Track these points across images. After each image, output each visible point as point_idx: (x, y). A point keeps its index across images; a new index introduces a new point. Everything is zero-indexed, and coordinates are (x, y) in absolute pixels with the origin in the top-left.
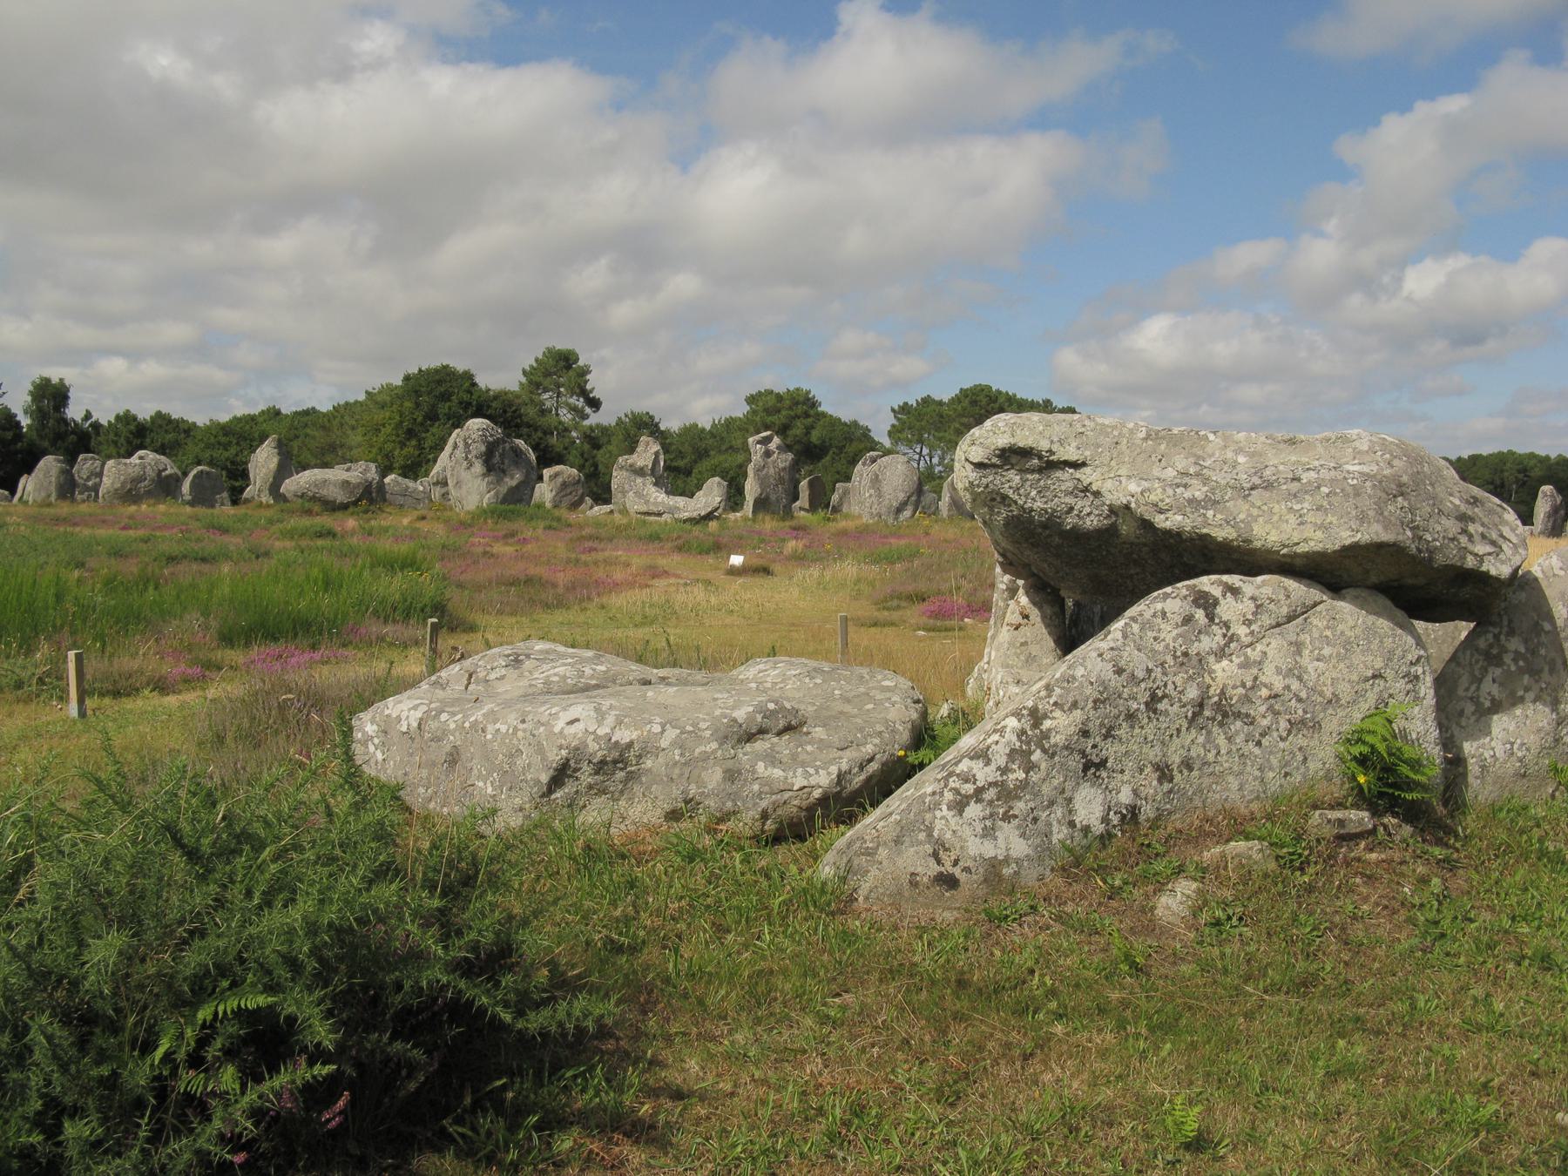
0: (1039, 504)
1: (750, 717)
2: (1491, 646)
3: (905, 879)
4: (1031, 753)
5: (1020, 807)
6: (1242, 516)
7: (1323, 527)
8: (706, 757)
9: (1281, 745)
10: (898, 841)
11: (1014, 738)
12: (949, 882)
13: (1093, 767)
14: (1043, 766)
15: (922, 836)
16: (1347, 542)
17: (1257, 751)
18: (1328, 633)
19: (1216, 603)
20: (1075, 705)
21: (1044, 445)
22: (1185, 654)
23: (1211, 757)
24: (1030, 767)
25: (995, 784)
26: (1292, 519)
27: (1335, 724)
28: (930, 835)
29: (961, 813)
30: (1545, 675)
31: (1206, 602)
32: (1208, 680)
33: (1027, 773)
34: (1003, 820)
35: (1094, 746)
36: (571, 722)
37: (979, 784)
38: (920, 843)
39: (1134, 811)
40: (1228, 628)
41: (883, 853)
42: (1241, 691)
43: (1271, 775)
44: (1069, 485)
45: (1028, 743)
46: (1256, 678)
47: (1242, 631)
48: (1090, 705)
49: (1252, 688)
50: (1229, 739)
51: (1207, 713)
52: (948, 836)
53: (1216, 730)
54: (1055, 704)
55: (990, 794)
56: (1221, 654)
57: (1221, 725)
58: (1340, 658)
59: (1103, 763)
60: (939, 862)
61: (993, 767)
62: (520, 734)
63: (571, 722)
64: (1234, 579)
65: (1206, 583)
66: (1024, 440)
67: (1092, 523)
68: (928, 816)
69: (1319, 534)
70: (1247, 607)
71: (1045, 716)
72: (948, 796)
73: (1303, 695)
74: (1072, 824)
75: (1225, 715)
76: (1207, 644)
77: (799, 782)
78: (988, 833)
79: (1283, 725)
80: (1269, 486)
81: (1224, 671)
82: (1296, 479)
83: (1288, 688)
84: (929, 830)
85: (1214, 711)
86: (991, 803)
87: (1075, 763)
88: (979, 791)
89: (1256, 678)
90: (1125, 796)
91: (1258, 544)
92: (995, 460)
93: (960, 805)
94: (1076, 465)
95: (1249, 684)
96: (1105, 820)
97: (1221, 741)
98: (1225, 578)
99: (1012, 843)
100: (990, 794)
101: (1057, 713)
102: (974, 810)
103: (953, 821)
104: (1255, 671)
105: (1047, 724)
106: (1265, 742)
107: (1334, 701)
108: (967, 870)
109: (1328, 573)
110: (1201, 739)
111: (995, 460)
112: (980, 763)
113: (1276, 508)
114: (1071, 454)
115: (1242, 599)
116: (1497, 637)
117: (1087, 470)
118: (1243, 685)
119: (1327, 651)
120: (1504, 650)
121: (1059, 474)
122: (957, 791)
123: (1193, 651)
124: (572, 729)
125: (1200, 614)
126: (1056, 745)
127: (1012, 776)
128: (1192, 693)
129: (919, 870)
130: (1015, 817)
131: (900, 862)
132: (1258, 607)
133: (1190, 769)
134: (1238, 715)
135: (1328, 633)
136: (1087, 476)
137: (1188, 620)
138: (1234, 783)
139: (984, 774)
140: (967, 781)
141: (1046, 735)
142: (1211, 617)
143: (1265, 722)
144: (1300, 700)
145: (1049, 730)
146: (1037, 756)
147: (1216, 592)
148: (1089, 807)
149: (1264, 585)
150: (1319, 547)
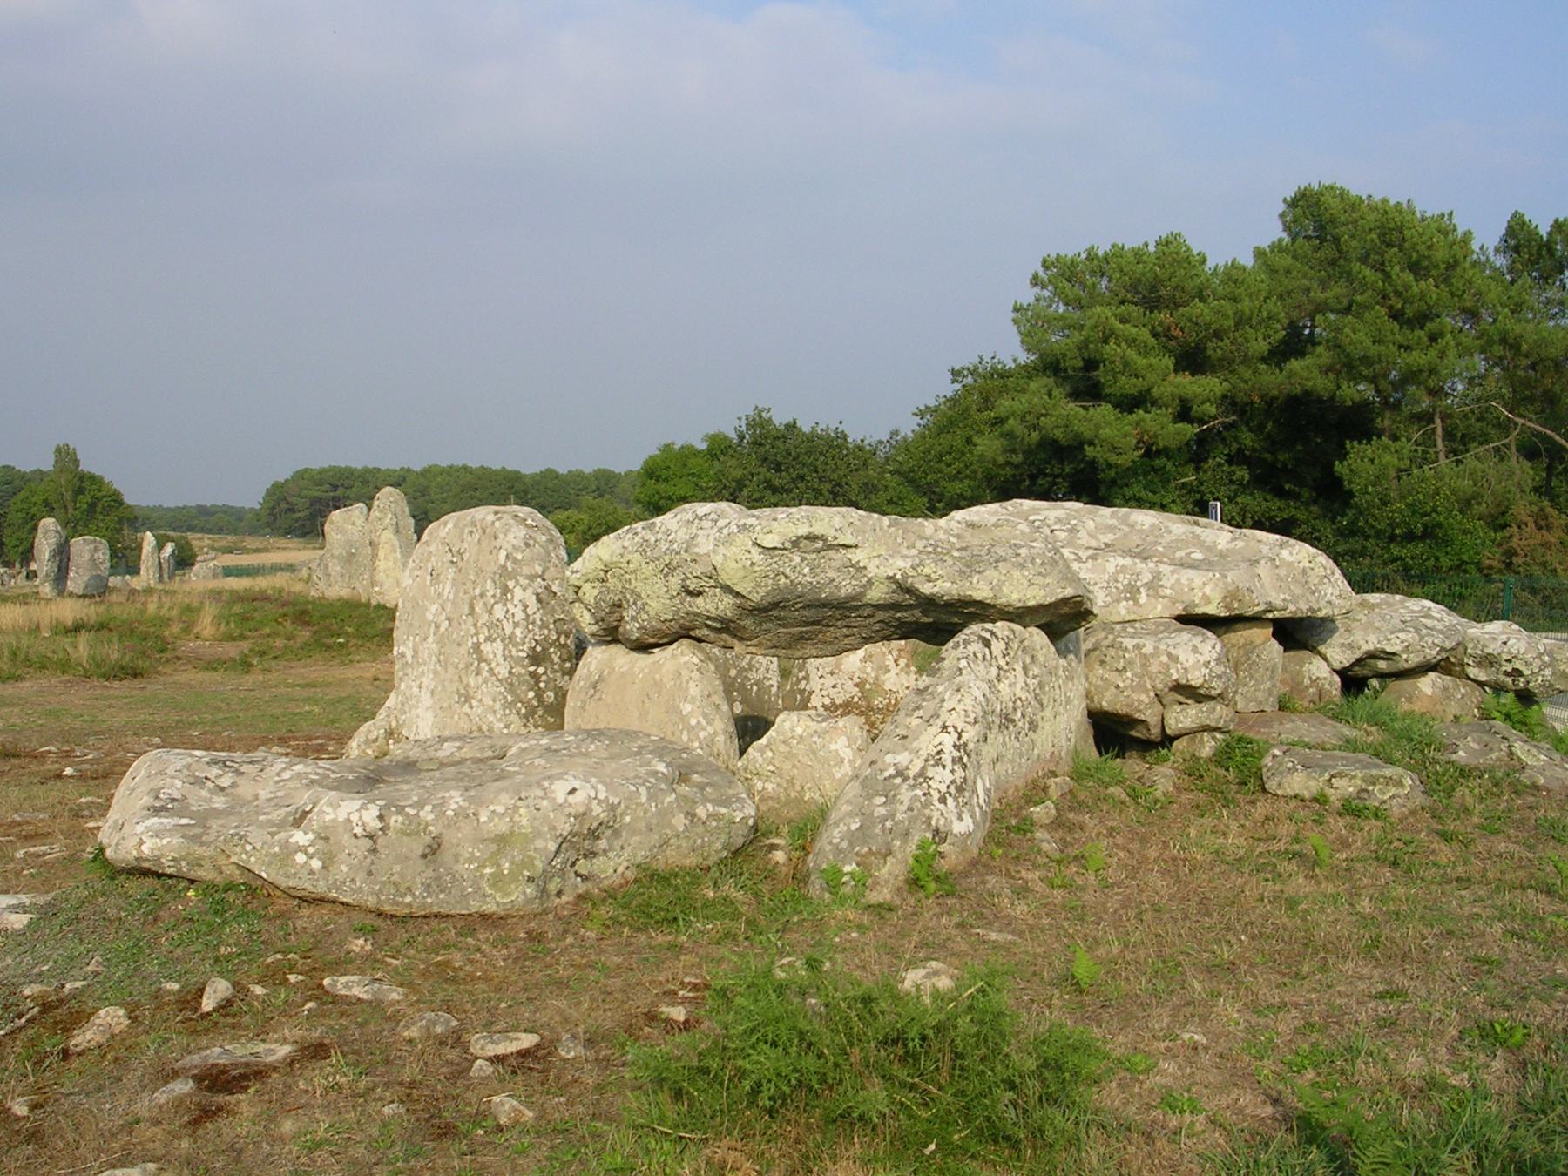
36: (573, 791)
47: (1002, 662)
63: (573, 791)
64: (989, 626)
65: (975, 628)
66: (817, 529)
70: (1002, 645)
72: (936, 795)
92: (788, 545)
105: (965, 736)
111: (788, 545)
121: (831, 553)
141: (965, 745)
147: (988, 635)
149: (1001, 627)
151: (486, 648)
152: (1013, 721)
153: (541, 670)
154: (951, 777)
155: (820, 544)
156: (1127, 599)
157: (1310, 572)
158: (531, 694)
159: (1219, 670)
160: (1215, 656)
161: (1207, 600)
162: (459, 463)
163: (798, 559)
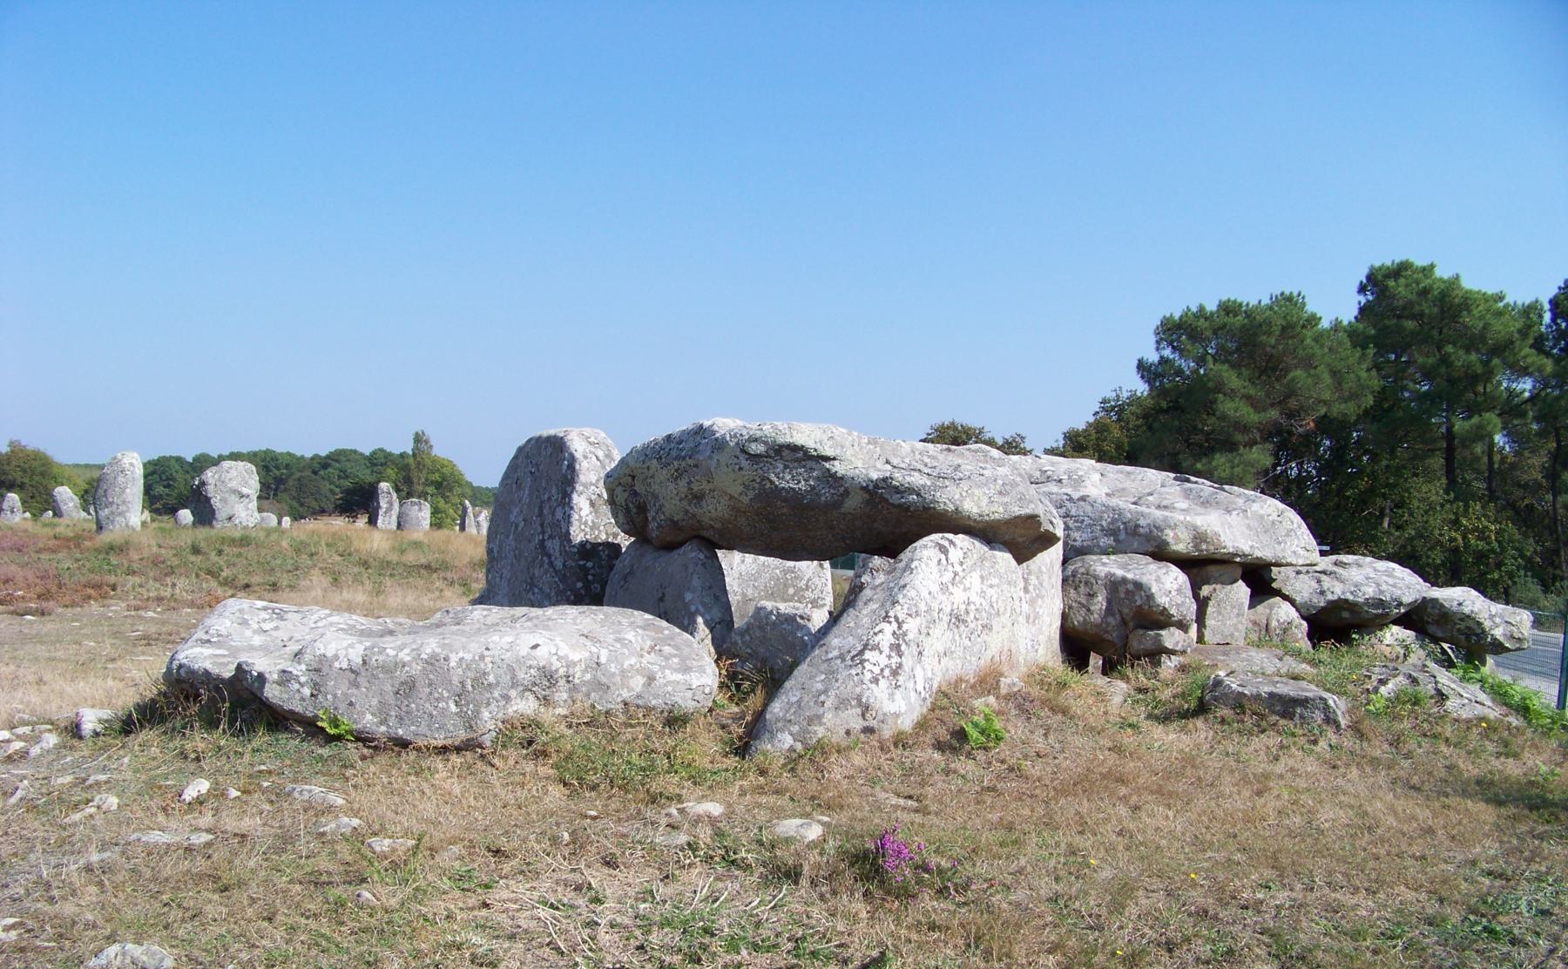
26: (986, 500)
36: (535, 647)
47: (958, 568)
55: (887, 672)
62: (488, 660)
63: (535, 647)
65: (936, 537)
70: (960, 554)
92: (771, 453)
93: (875, 681)
94: (827, 459)
105: (905, 627)
111: (771, 453)
117: (836, 463)
121: (810, 464)
124: (534, 652)
141: (905, 634)
146: (903, 647)
147: (946, 544)
149: (961, 540)
151: (548, 544)
152: (964, 621)
153: (590, 564)
154: (887, 662)
155: (800, 454)
158: (579, 585)
159: (1179, 600)
161: (1177, 539)
162: (658, 434)
163: (781, 466)
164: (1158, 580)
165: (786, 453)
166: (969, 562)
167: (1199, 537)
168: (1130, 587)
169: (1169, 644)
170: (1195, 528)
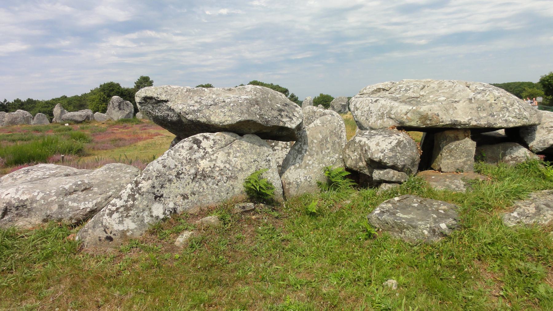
0: (159, 114)
1: (71, 187)
2: (299, 148)
3: (98, 239)
4: (135, 195)
5: (132, 213)
6: (207, 114)
7: (231, 116)
8: (52, 201)
9: (225, 184)
10: (94, 227)
11: (130, 191)
12: (110, 239)
13: (158, 198)
14: (139, 199)
15: (100, 225)
16: (238, 121)
17: (217, 187)
18: (238, 149)
19: (201, 142)
20: (149, 179)
21: (155, 96)
22: (190, 159)
23: (201, 190)
24: (134, 200)
25: (123, 206)
26: (222, 114)
27: (242, 177)
28: (102, 224)
29: (111, 217)
30: (315, 156)
31: (197, 142)
32: (198, 166)
33: (134, 201)
34: (126, 217)
35: (158, 191)
37: (118, 207)
38: (100, 227)
39: (175, 210)
40: (205, 150)
41: (90, 231)
42: (210, 169)
43: (222, 194)
44: (165, 108)
45: (134, 192)
46: (214, 165)
47: (210, 150)
48: (154, 178)
49: (213, 168)
50: (207, 184)
51: (198, 177)
52: (107, 224)
53: (202, 182)
54: (143, 179)
56: (203, 158)
57: (204, 180)
58: (242, 156)
59: (162, 196)
60: (106, 233)
61: (123, 200)
64: (207, 134)
65: (199, 136)
67: (175, 119)
68: (101, 218)
69: (230, 119)
70: (211, 142)
71: (140, 183)
73: (231, 169)
74: (152, 216)
75: (205, 177)
76: (197, 155)
77: (82, 207)
78: (121, 222)
79: (225, 178)
80: (216, 104)
81: (204, 164)
82: (224, 102)
83: (225, 167)
84: (102, 223)
85: (201, 176)
86: (121, 212)
87: (152, 197)
88: (117, 209)
89: (214, 165)
90: (171, 205)
91: (213, 123)
93: (111, 214)
94: (166, 101)
95: (212, 167)
96: (164, 213)
97: (204, 185)
98: (205, 134)
99: (130, 225)
100: (122, 209)
101: (143, 182)
102: (116, 215)
103: (108, 220)
104: (214, 162)
105: (140, 185)
106: (219, 184)
107: (242, 170)
108: (114, 235)
109: (239, 130)
110: (197, 185)
112: (119, 200)
113: (217, 111)
114: (163, 97)
115: (208, 141)
116: (301, 145)
117: (169, 103)
118: (210, 167)
119: (238, 154)
120: (302, 149)
121: (161, 104)
122: (110, 210)
123: (193, 158)
124: (7, 197)
125: (195, 146)
126: (143, 192)
127: (129, 203)
128: (193, 171)
129: (101, 236)
130: (130, 216)
131: (95, 234)
132: (215, 142)
133: (195, 194)
134: (209, 177)
135: (238, 149)
136: (170, 104)
137: (191, 148)
138: (210, 198)
139: (119, 203)
140: (113, 206)
141: (140, 189)
142: (199, 147)
143: (219, 178)
144: (229, 170)
145: (141, 187)
146: (137, 196)
148: (158, 210)
149: (217, 136)
150: (230, 123)
156: (381, 119)
157: (494, 105)
160: (390, 147)
161: (411, 120)
164: (378, 144)
165: (148, 101)
166: (217, 146)
167: (424, 117)
168: (366, 148)
169: (386, 178)
170: (419, 113)
